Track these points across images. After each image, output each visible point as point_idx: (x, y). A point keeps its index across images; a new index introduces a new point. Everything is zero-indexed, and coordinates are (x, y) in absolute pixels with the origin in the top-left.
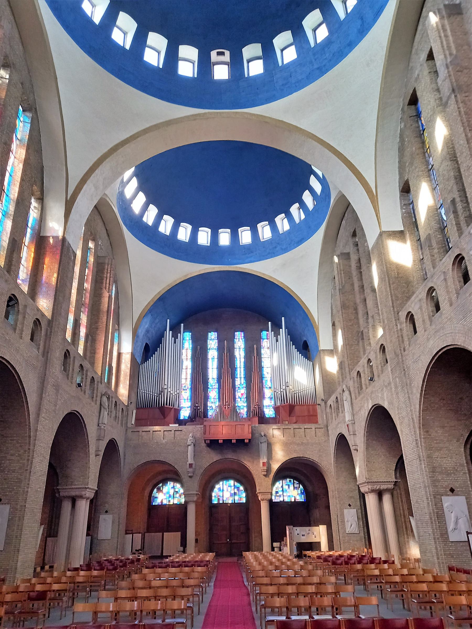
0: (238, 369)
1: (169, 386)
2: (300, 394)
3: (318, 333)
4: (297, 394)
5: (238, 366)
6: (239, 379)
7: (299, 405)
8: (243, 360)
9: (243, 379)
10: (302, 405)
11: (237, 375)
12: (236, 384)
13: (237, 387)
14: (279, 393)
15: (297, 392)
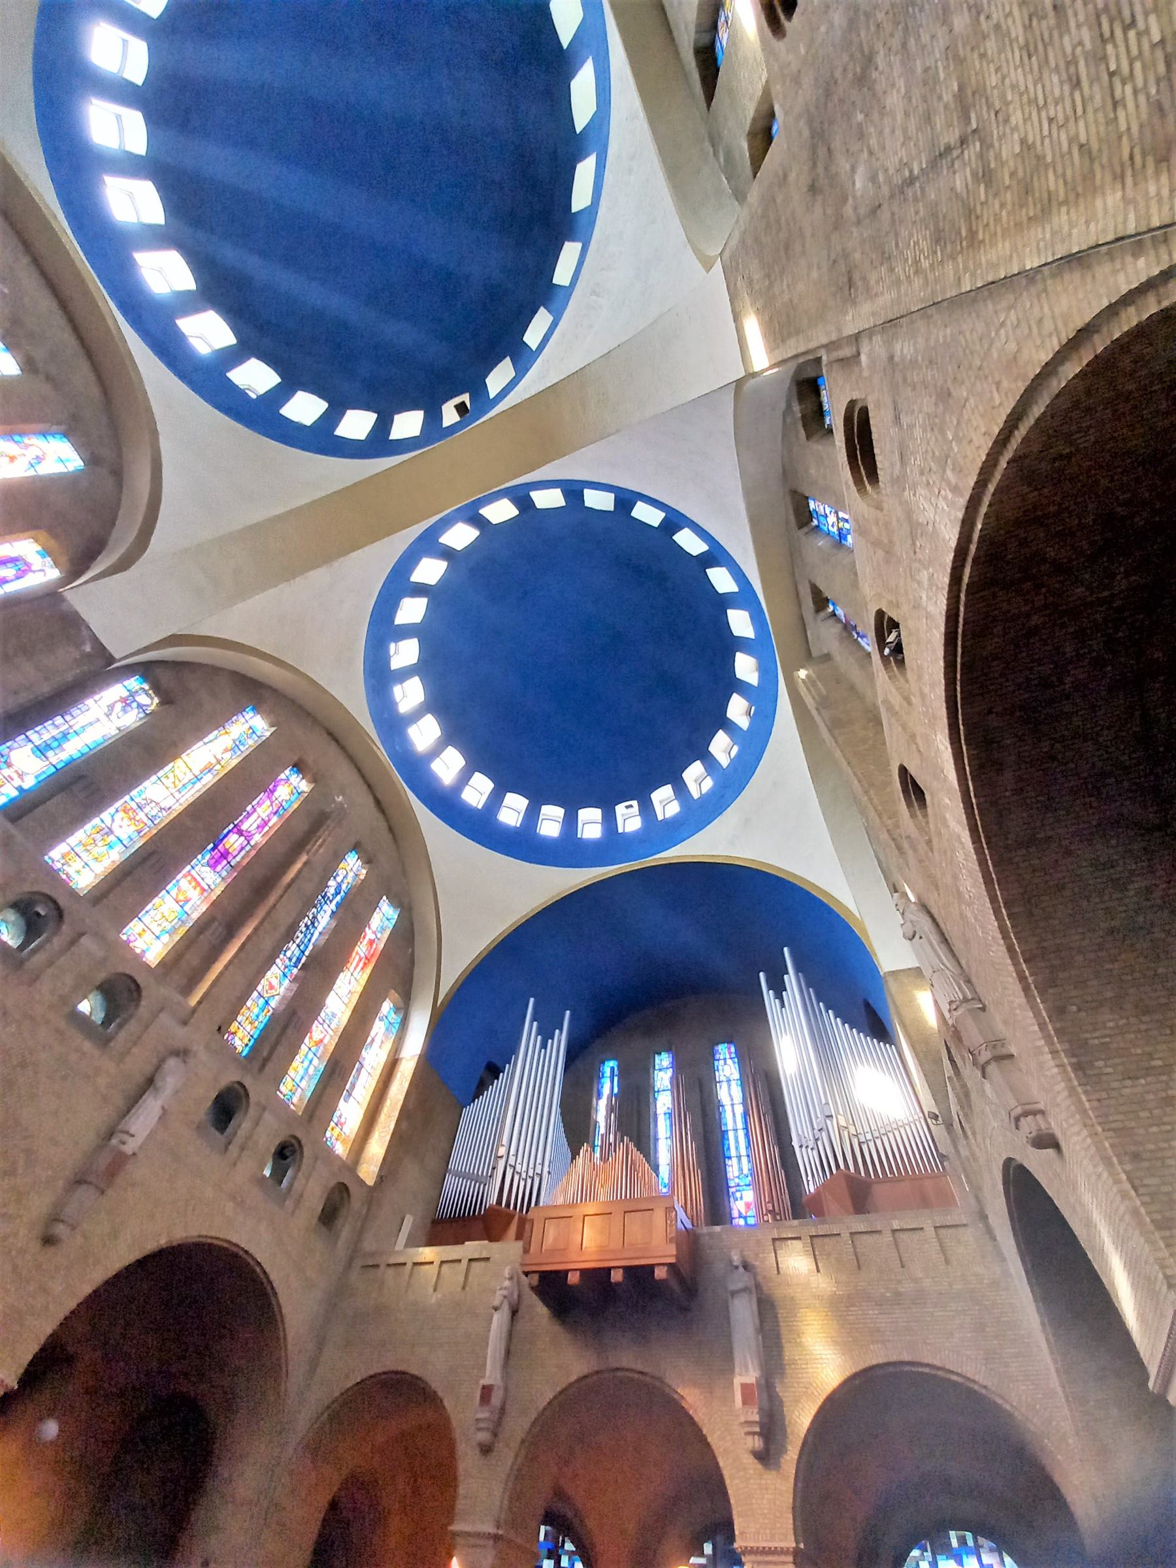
0: (731, 1135)
1: (512, 1151)
2: (879, 1142)
3: (871, 945)
4: (872, 1145)
5: (730, 1126)
6: (735, 1160)
7: (886, 1180)
8: (739, 1109)
9: (744, 1160)
10: (894, 1180)
11: (729, 1149)
12: (730, 1175)
13: (731, 1184)
14: (811, 1144)
15: (869, 1136)
